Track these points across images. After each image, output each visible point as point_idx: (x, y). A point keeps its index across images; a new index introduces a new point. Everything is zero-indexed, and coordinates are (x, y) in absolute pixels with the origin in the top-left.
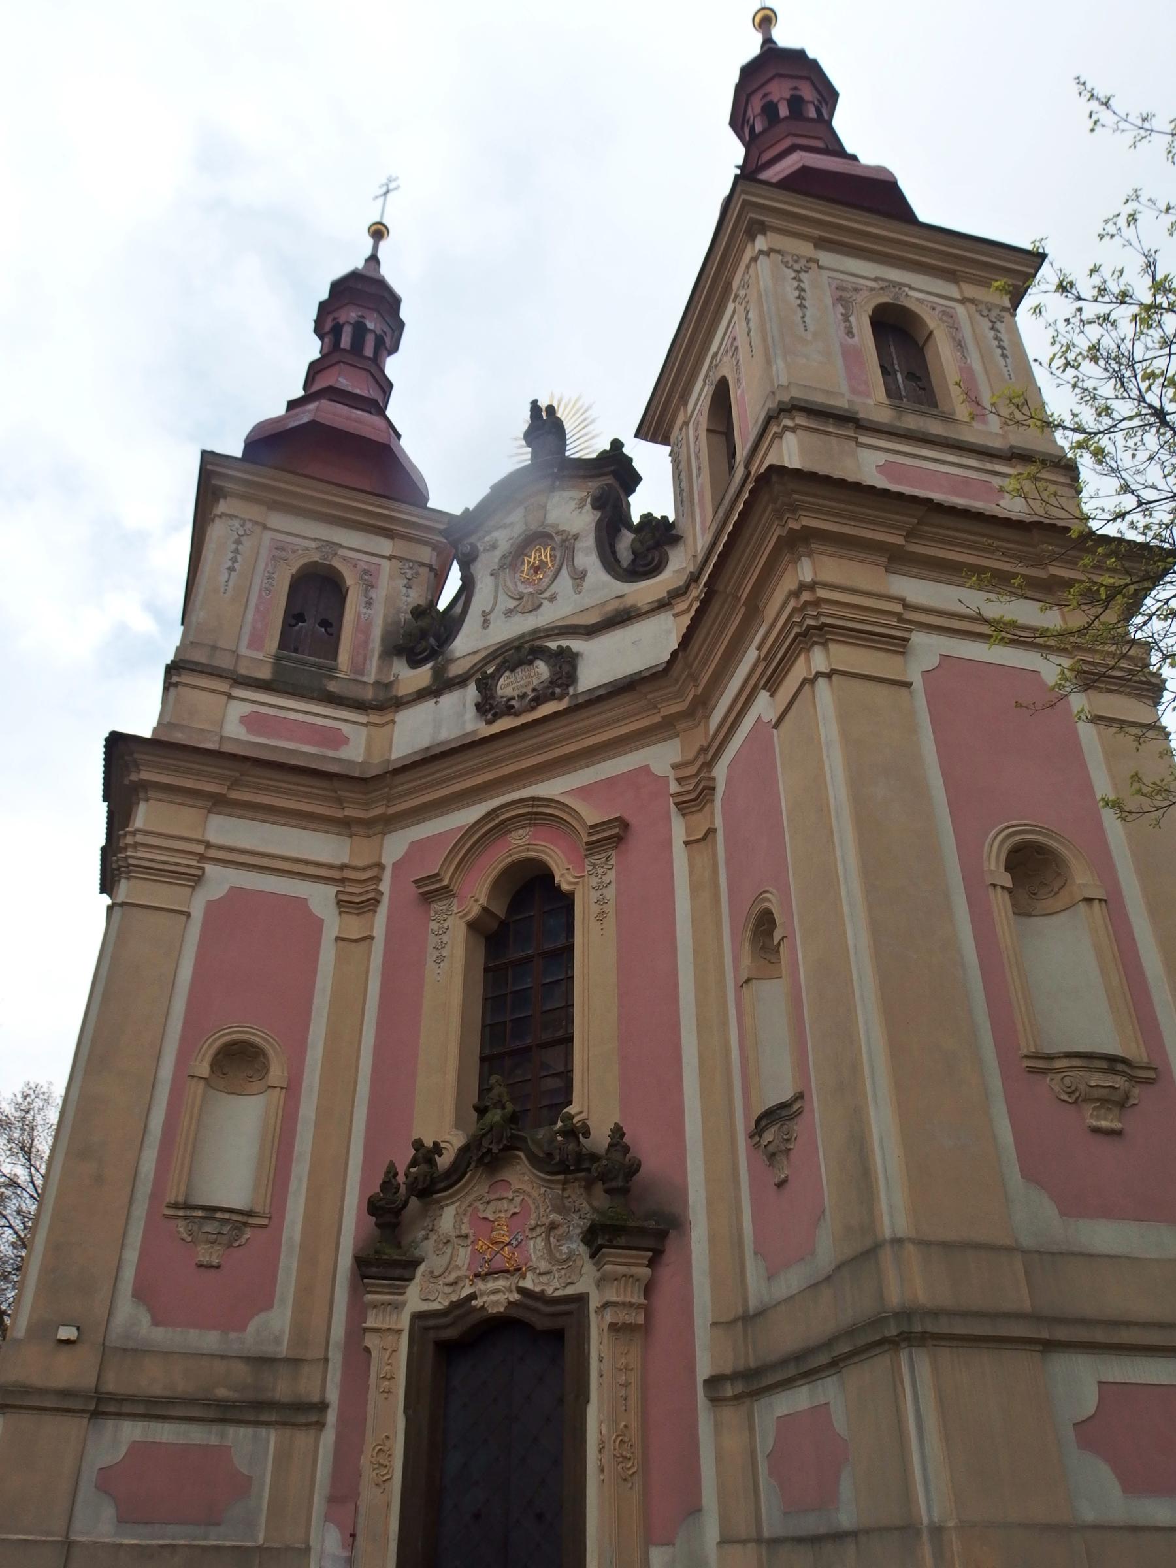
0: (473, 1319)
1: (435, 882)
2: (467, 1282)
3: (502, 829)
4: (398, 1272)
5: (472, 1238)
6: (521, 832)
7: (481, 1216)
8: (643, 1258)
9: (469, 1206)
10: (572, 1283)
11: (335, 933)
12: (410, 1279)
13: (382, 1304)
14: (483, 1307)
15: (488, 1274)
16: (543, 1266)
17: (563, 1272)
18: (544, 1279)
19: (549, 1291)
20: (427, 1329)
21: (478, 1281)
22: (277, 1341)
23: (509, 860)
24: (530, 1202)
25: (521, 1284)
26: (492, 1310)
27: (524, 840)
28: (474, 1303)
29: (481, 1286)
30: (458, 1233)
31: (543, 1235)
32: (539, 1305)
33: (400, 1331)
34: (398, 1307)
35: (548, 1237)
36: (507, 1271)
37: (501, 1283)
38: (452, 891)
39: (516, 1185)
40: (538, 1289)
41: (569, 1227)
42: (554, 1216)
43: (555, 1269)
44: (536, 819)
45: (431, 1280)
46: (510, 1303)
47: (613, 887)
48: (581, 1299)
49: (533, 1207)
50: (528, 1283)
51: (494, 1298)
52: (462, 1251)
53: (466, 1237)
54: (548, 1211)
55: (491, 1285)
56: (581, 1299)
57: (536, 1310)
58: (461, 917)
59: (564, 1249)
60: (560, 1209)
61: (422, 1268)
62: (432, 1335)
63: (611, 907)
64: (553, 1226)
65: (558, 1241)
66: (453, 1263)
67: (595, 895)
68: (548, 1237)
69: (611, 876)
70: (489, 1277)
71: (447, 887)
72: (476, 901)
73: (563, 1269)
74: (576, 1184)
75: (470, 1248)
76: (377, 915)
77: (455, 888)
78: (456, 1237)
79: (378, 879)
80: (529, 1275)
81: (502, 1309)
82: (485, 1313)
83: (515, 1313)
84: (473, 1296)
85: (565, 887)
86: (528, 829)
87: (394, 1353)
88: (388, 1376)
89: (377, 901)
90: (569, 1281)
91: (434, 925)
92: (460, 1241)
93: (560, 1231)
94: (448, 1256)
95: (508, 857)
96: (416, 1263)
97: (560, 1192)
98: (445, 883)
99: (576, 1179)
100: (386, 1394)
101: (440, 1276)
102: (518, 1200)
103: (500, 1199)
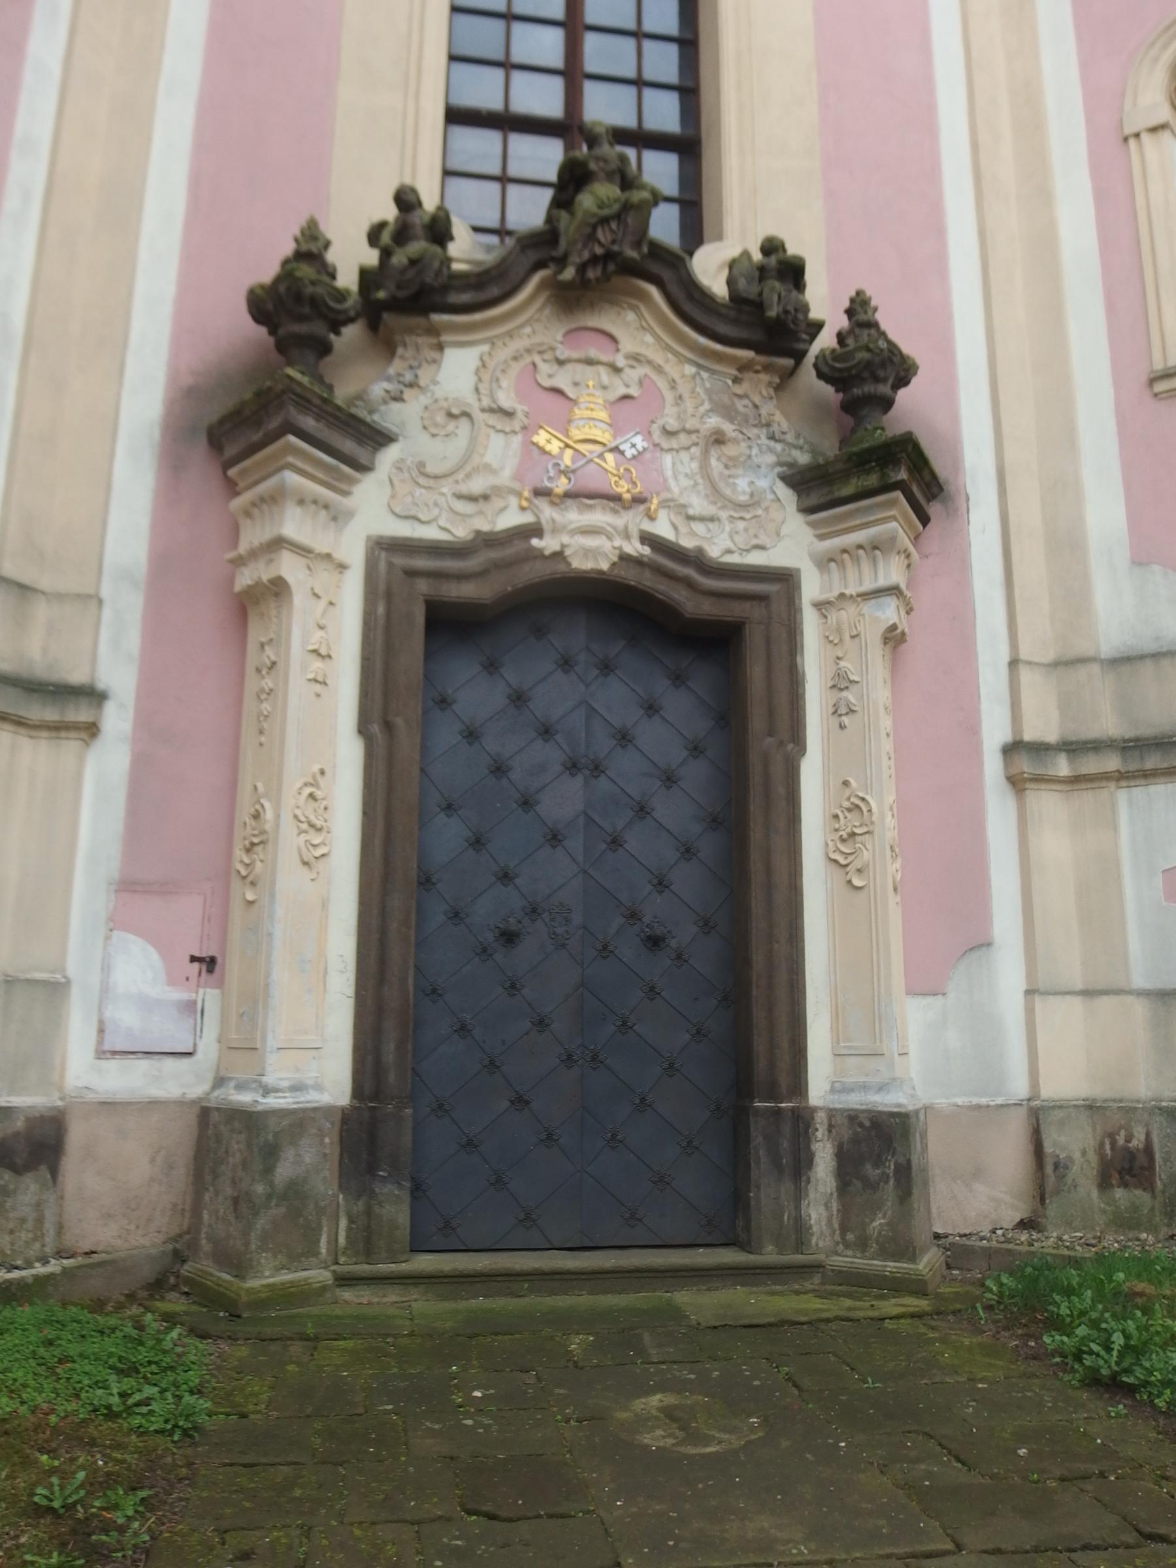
0: (529, 574)
4: (348, 446)
7: (547, 383)
9: (515, 358)
12: (364, 468)
13: (315, 502)
14: (559, 555)
15: (568, 495)
17: (741, 525)
18: (699, 527)
19: (714, 552)
20: (411, 574)
21: (543, 505)
24: (662, 384)
25: (648, 526)
26: (580, 564)
28: (535, 542)
29: (547, 513)
30: (486, 402)
34: (338, 517)
36: (616, 498)
37: (599, 517)
40: (687, 543)
41: (750, 447)
42: (714, 421)
43: (724, 515)
46: (624, 558)
48: (786, 579)
49: (669, 396)
50: (663, 528)
55: (573, 516)
57: (689, 583)
60: (729, 413)
62: (423, 586)
64: (719, 439)
66: (476, 460)
70: (569, 502)
73: (742, 518)
74: (765, 377)
78: (483, 410)
80: (663, 516)
81: (605, 566)
83: (648, 581)
84: (536, 530)
90: (755, 542)
93: (730, 450)
97: (730, 382)
99: (767, 368)
103: (590, 362)
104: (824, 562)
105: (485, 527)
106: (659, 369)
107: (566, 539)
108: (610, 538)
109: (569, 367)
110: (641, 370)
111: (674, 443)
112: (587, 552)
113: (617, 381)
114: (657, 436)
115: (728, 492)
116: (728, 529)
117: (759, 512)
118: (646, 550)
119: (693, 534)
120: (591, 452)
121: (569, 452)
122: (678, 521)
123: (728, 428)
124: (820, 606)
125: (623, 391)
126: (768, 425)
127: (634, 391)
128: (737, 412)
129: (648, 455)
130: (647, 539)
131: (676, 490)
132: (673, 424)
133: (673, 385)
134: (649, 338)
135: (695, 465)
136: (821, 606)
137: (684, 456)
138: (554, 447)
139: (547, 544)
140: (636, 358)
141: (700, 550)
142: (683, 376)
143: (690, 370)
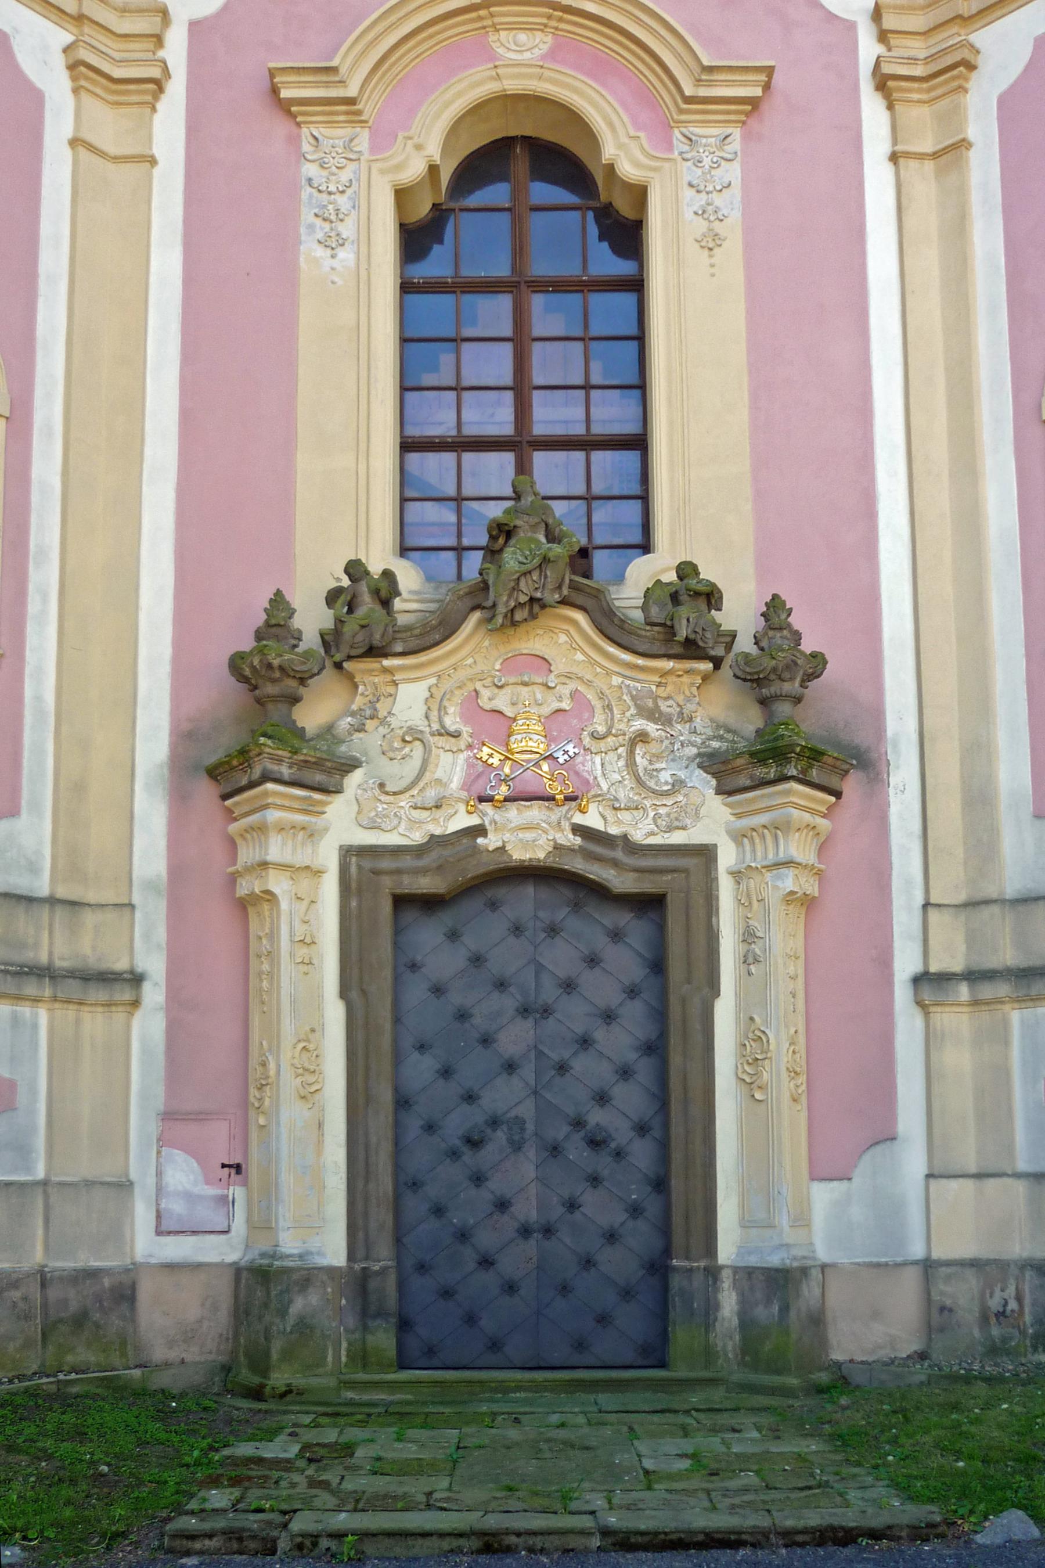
1: (327, 84)
2: (462, 808)
3: (481, 18)
5: (466, 738)
6: (522, 37)
8: (822, 802)
10: (684, 828)
11: (68, 130)
14: (502, 849)
15: (507, 799)
16: (625, 793)
17: (662, 811)
19: (638, 836)
21: (486, 807)
22: (33, 869)
23: (490, 88)
25: (579, 819)
26: (519, 855)
27: (527, 55)
28: (480, 841)
31: (621, 750)
32: (619, 854)
33: (318, 873)
34: (312, 835)
35: (631, 753)
36: (551, 798)
37: (535, 812)
38: (359, 113)
39: (560, 666)
40: (613, 830)
41: (673, 744)
42: (639, 724)
43: (648, 803)
44: (560, 20)
45: (383, 798)
46: (557, 847)
47: (736, 191)
48: (706, 853)
49: (597, 704)
50: (592, 819)
51: (529, 835)
52: (446, 758)
53: (456, 735)
54: (628, 714)
55: (514, 814)
56: (706, 853)
58: (382, 172)
59: (665, 776)
60: (653, 715)
61: (355, 779)
63: (732, 229)
64: (642, 737)
65: (651, 762)
67: (689, 198)
68: (631, 753)
69: (733, 172)
71: (351, 101)
72: (419, 147)
75: (462, 757)
76: (157, 118)
77: (368, 108)
79: (158, 40)
80: (593, 808)
81: (541, 855)
82: (505, 858)
84: (480, 831)
85: (628, 170)
86: (539, 34)
87: (313, 904)
88: (308, 940)
89: (158, 85)
90: (676, 824)
91: (310, 170)
92: (441, 741)
93: (654, 748)
94: (416, 762)
95: (492, 78)
96: (350, 765)
97: (654, 688)
98: (352, 91)
100: (306, 967)
101: (401, 793)
102: (565, 691)
103: (525, 684)
104: (739, 837)
105: (438, 832)
106: (588, 683)
107: (507, 836)
108: (545, 832)
109: (507, 690)
110: (572, 685)
111: (602, 745)
112: (525, 845)
113: (550, 697)
114: (587, 741)
115: (652, 784)
116: (652, 814)
117: (680, 798)
118: (578, 841)
119: (619, 822)
120: (528, 761)
121: (509, 763)
122: (609, 814)
123: (651, 728)
124: (736, 875)
125: (556, 705)
126: (691, 720)
127: (566, 705)
128: (661, 713)
129: (579, 759)
130: (579, 830)
131: (605, 786)
132: (601, 729)
133: (601, 695)
134: (580, 657)
135: (621, 763)
136: (736, 875)
137: (612, 756)
138: (495, 761)
139: (490, 842)
140: (568, 676)
141: (625, 837)
142: (611, 687)
143: (616, 680)
